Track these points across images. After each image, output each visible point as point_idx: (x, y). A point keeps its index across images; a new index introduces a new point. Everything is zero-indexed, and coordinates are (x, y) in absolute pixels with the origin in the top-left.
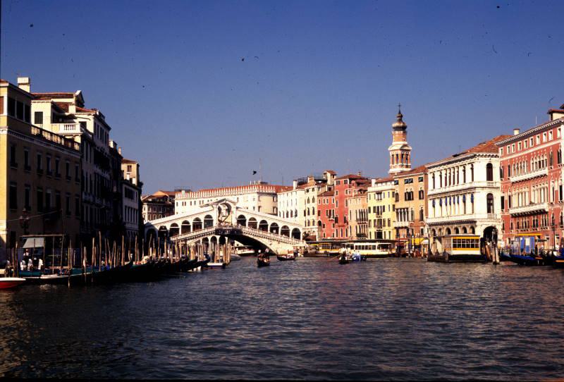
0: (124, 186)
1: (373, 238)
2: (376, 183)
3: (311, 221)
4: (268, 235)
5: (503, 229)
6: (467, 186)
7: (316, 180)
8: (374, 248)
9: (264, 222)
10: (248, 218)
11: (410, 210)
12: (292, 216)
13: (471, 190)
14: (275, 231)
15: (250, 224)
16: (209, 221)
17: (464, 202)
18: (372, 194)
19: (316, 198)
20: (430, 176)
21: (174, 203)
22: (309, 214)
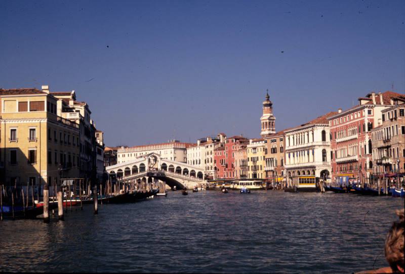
0: (97, 147)
1: (251, 177)
2: (253, 142)
3: (210, 167)
4: (182, 176)
5: (332, 171)
6: (310, 144)
7: (213, 140)
8: (251, 184)
9: (179, 167)
10: (168, 165)
11: (274, 159)
12: (197, 163)
13: (312, 148)
14: (186, 174)
15: (170, 169)
16: (143, 168)
17: (308, 154)
18: (250, 149)
19: (213, 152)
20: (287, 138)
21: (116, 155)
22: (208, 162)
